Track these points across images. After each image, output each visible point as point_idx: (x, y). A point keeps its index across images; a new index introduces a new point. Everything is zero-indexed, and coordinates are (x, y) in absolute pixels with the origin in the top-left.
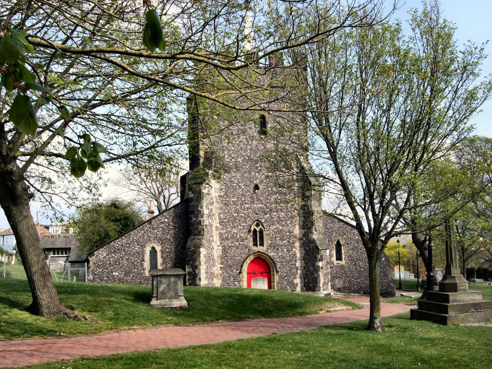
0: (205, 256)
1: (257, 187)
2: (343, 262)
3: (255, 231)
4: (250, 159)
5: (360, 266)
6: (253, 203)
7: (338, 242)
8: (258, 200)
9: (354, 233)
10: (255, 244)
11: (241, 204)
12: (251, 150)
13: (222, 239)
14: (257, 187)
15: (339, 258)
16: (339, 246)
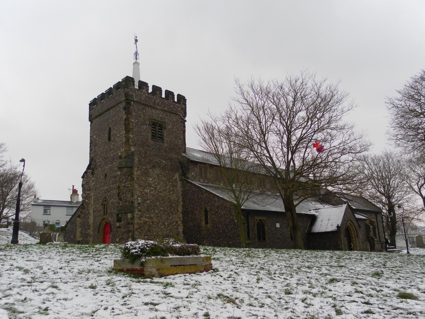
0: (80, 223)
1: (106, 175)
2: (209, 225)
3: (105, 205)
4: (105, 158)
5: (219, 229)
6: (104, 186)
7: (206, 209)
8: (106, 183)
9: (215, 200)
10: (104, 215)
11: (100, 188)
12: (105, 152)
13: (94, 212)
14: (106, 175)
15: (207, 223)
16: (206, 211)
